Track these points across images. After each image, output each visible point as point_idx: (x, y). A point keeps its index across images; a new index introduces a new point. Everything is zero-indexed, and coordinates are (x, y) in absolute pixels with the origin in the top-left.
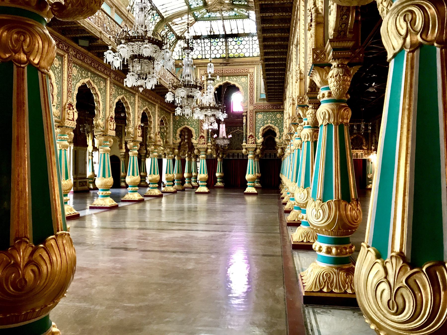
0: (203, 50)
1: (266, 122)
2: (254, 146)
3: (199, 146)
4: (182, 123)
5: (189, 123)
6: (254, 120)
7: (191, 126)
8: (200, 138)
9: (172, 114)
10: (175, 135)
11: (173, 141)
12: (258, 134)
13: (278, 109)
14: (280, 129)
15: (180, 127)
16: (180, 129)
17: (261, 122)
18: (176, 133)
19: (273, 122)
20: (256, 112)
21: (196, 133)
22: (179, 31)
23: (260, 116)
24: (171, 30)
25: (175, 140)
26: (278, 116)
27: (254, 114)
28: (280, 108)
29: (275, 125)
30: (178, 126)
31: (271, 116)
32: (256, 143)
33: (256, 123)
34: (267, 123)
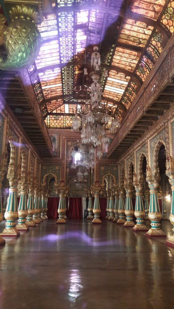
0: (65, 122)
1: (106, 172)
2: (99, 188)
3: (59, 188)
4: (48, 171)
5: (53, 172)
6: (99, 171)
7: (54, 174)
8: (61, 182)
9: (40, 165)
10: (43, 180)
11: (40, 184)
12: (102, 181)
13: (115, 164)
14: (116, 177)
15: (46, 174)
16: (46, 175)
17: (104, 172)
18: (43, 178)
19: (111, 172)
20: (100, 165)
21: (58, 179)
22: (50, 109)
23: (102, 168)
24: (46, 108)
25: (42, 184)
26: (115, 169)
27: (99, 166)
28: (116, 164)
29: (113, 175)
30: (45, 174)
31: (110, 168)
32: (101, 187)
33: (100, 173)
34: (108, 173)
